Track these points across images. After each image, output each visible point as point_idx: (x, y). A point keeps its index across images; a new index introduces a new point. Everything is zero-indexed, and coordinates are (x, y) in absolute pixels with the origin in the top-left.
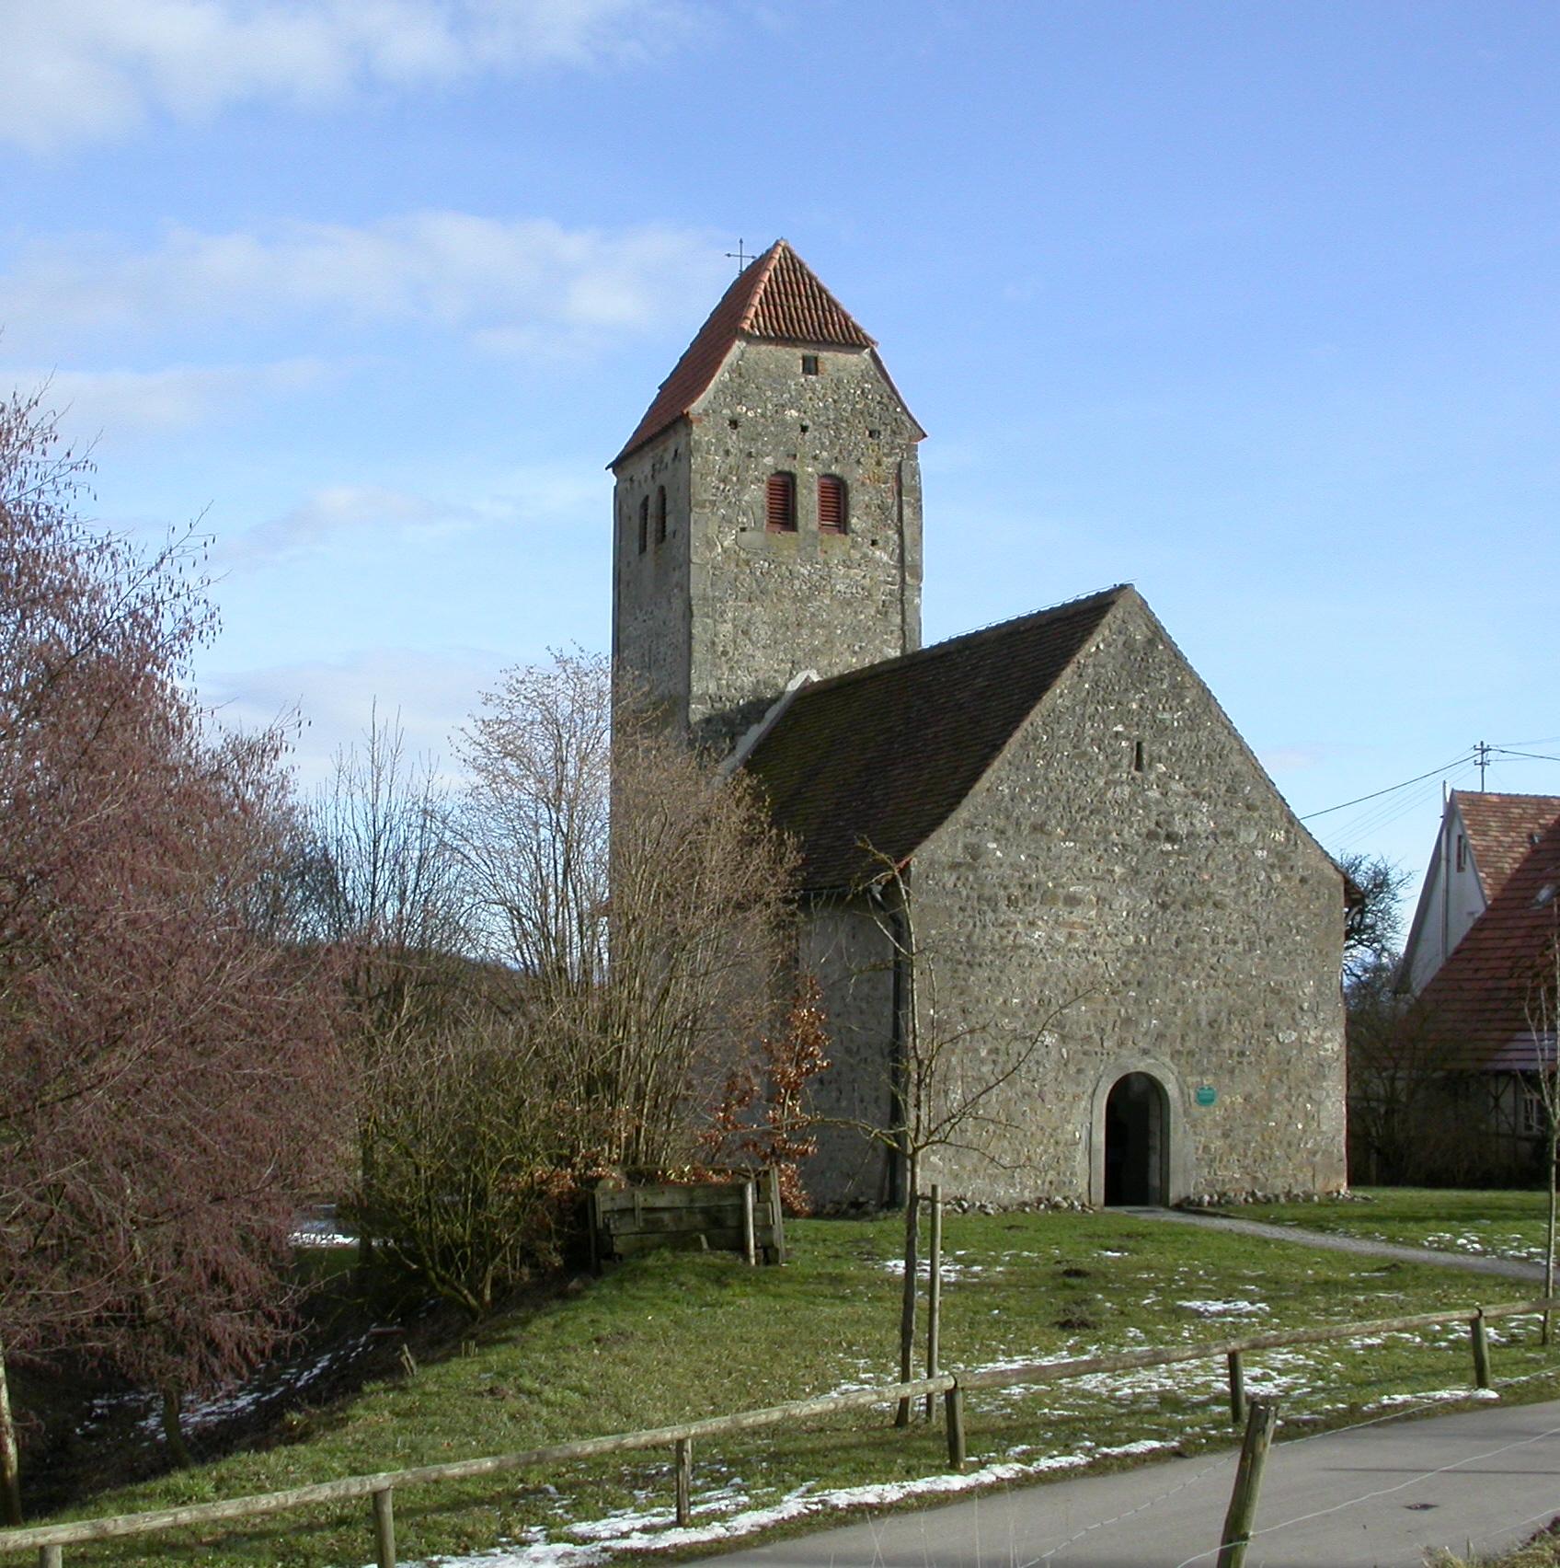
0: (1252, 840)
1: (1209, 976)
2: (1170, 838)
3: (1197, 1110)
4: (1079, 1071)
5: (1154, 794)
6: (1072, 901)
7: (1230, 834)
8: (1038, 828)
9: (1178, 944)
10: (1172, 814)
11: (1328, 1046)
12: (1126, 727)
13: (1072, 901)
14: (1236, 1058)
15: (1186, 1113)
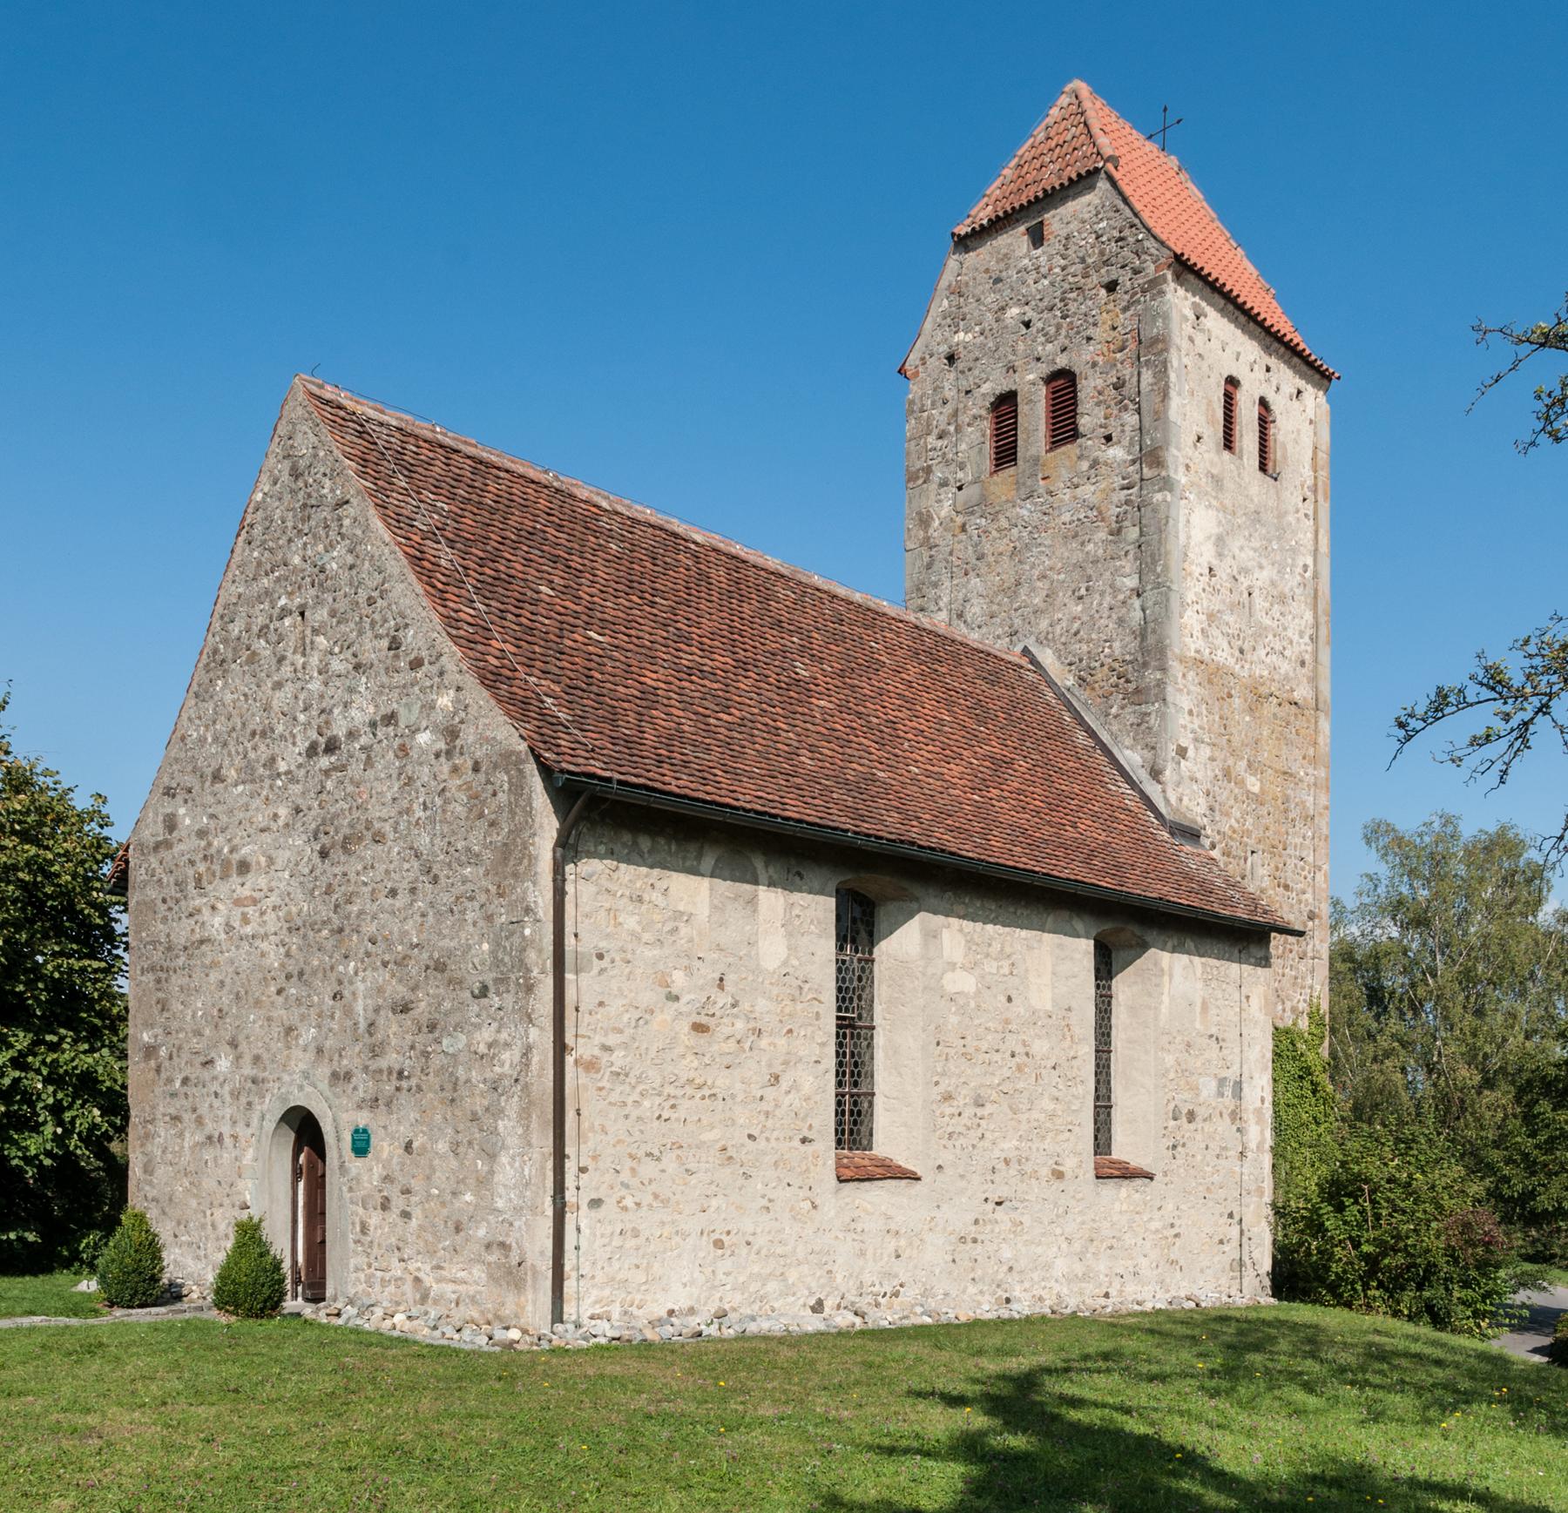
0: (413, 719)
1: (368, 954)
2: (331, 747)
4: (249, 1104)
5: (315, 686)
6: (244, 867)
8: (217, 777)
9: (336, 906)
11: (506, 1056)
13: (244, 867)
15: (342, 1166)
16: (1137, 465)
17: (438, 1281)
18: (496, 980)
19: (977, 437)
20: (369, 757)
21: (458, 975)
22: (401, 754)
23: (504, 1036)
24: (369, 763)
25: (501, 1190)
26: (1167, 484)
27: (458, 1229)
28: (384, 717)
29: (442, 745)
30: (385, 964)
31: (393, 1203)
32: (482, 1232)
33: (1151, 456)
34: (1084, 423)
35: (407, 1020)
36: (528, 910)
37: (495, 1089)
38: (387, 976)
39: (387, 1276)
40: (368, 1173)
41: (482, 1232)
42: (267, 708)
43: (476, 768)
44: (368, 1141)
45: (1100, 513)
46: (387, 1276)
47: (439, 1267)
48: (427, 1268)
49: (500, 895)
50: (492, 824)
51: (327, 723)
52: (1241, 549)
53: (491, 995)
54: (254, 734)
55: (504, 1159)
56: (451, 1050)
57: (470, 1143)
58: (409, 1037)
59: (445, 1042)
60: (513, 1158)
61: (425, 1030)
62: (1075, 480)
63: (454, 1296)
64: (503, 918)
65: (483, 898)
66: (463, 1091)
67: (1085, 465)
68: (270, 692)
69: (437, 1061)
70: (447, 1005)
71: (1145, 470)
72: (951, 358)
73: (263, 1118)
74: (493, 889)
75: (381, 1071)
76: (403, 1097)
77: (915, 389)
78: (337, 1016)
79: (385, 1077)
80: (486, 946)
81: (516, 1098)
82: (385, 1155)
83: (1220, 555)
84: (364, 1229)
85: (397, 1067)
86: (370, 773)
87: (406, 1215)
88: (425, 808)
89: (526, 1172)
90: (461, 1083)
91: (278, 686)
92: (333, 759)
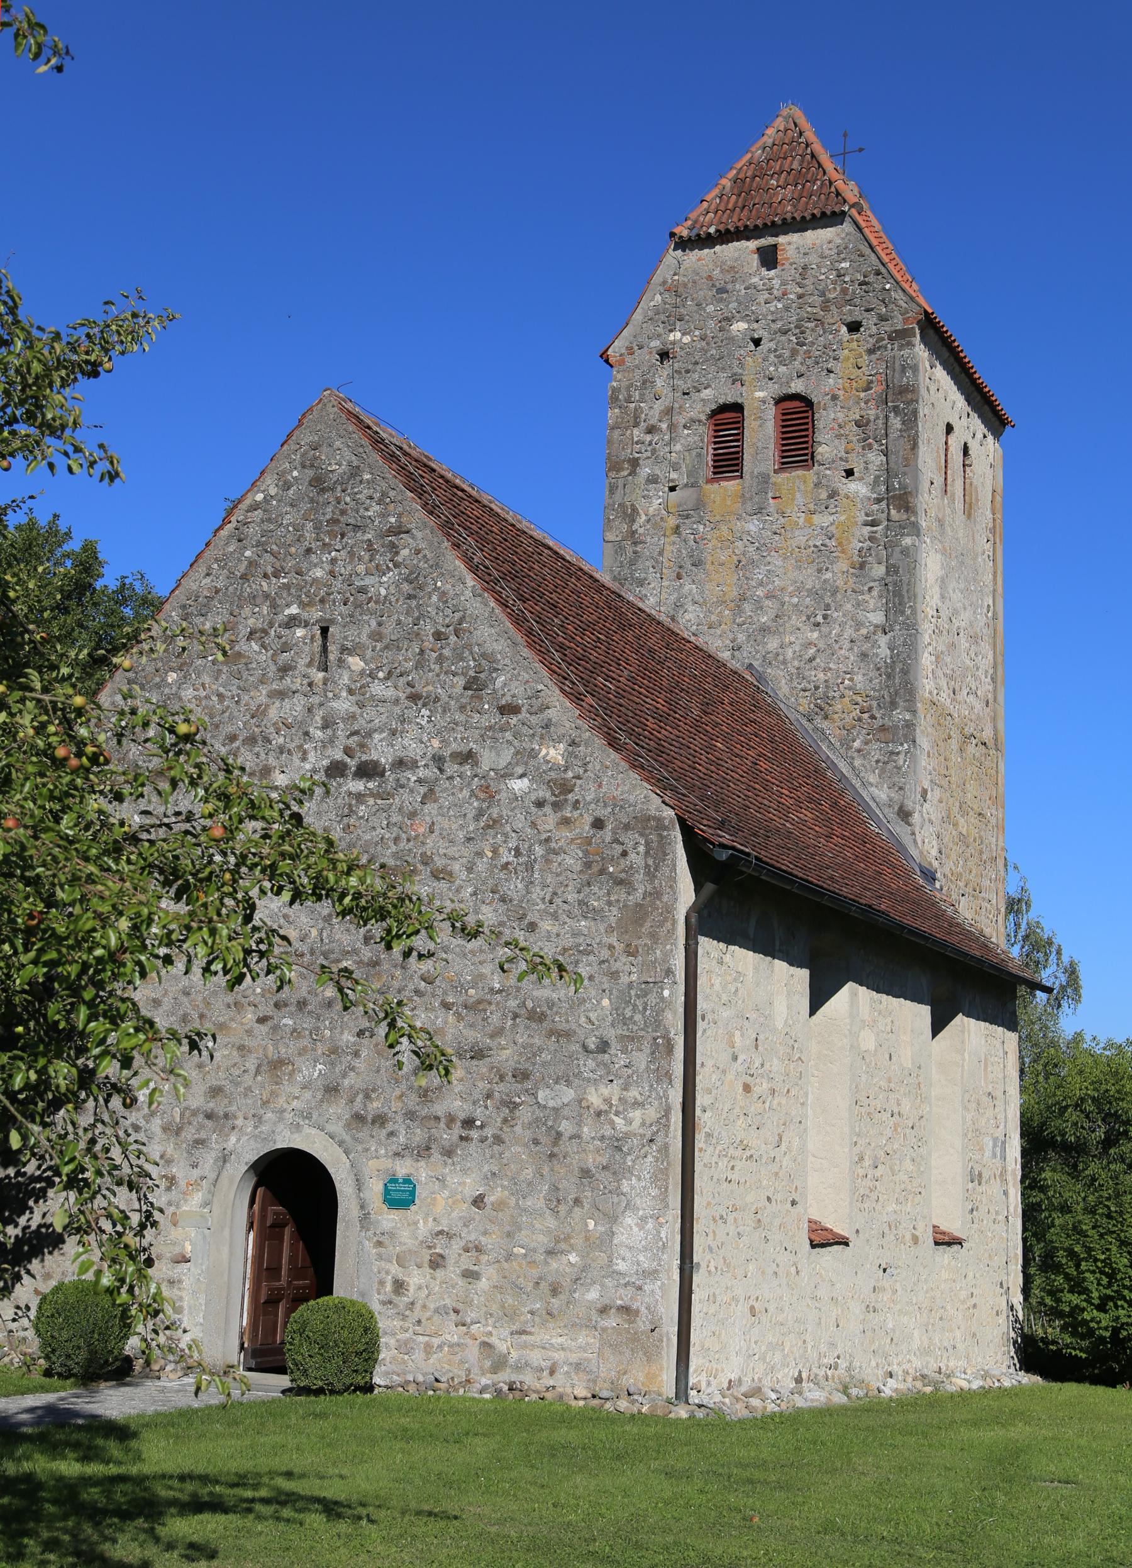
0: (503, 763)
1: (417, 992)
2: (367, 771)
3: (389, 1219)
5: (343, 705)
7: (468, 757)
10: (369, 734)
12: (302, 605)
14: (457, 1130)
16: (884, 504)
17: (525, 1346)
18: (621, 1038)
19: (693, 441)
20: (431, 791)
21: (563, 1026)
22: (482, 796)
23: (633, 1093)
24: (429, 796)
25: (623, 1251)
26: (915, 530)
27: (555, 1291)
28: (455, 755)
29: (544, 793)
30: (446, 1006)
31: (450, 1262)
32: (593, 1295)
33: (899, 498)
34: (823, 451)
35: (482, 1067)
36: (669, 972)
37: (619, 1149)
38: (451, 1019)
39: (436, 1341)
40: (410, 1228)
41: (593, 1295)
42: (259, 713)
43: (598, 824)
44: (413, 1193)
45: (840, 544)
46: (436, 1341)
47: (523, 1332)
48: (505, 1333)
49: (630, 954)
50: (620, 882)
51: (362, 746)
52: (954, 591)
53: (613, 1051)
54: (233, 738)
55: (629, 1220)
56: (551, 1104)
57: (577, 1201)
58: (483, 1086)
59: (541, 1095)
60: (644, 1219)
61: (509, 1078)
62: (812, 507)
63: (549, 1363)
64: (634, 977)
65: (605, 954)
66: (565, 1146)
67: (824, 495)
68: (263, 699)
69: (525, 1114)
70: (546, 1056)
71: (893, 512)
72: (664, 355)
73: (224, 1158)
74: (619, 947)
75: (437, 1118)
76: (472, 1147)
77: (618, 379)
78: (364, 1054)
79: (442, 1125)
80: (606, 1002)
81: (650, 1159)
82: (440, 1208)
83: (943, 597)
84: (399, 1286)
85: (462, 1115)
86: (430, 808)
87: (470, 1275)
88: (518, 852)
89: (663, 1235)
90: (565, 1138)
91: (281, 695)
92: (371, 785)
